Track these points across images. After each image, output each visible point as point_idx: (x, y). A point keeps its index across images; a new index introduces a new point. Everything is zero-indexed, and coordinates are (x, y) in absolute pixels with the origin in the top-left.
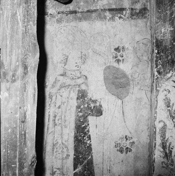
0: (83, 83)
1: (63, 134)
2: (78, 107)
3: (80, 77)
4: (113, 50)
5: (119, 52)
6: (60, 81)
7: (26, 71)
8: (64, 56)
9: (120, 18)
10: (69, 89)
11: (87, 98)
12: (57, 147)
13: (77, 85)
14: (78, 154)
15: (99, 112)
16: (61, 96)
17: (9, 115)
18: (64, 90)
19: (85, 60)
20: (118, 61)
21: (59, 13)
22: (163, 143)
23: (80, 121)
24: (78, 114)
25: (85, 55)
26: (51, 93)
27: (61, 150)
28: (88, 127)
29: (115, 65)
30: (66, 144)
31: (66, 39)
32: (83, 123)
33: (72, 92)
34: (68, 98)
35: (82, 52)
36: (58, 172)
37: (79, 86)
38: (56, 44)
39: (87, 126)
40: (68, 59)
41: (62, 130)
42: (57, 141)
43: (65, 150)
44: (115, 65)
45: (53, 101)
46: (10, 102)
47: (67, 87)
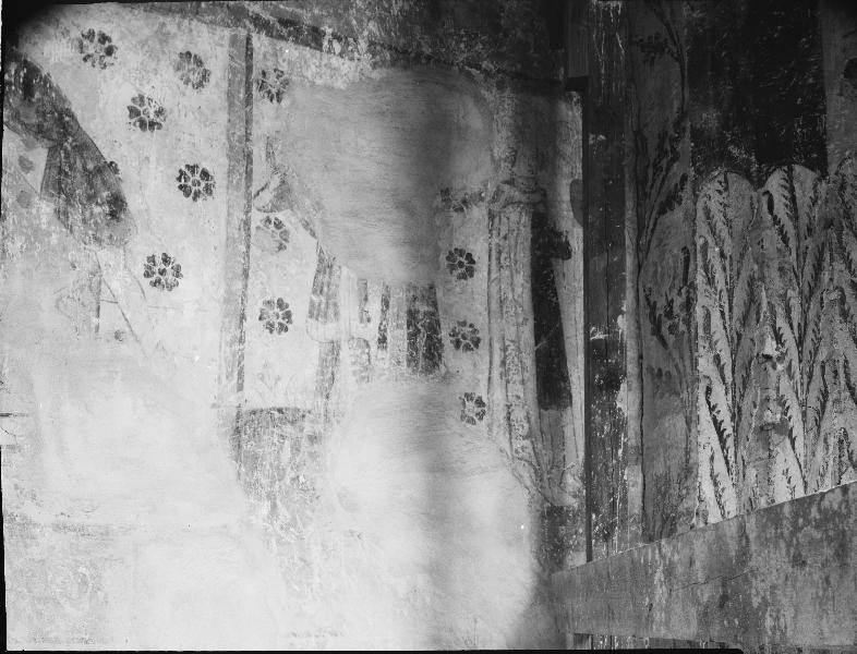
16: (508, 219)
30: (520, 300)
36: (512, 347)
43: (519, 310)
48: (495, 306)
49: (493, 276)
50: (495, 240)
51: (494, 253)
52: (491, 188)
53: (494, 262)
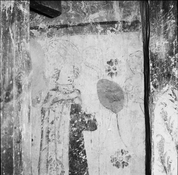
0: (76, 97)
1: (58, 150)
2: (72, 122)
3: (73, 92)
4: (106, 64)
5: (112, 65)
6: (52, 95)
7: (20, 89)
8: (56, 70)
9: (112, 31)
10: (62, 104)
11: (81, 113)
12: (51, 164)
13: (70, 99)
14: (74, 170)
15: (93, 126)
16: (54, 111)
17: (3, 135)
18: (56, 105)
19: (77, 74)
20: (112, 74)
21: (49, 27)
22: (161, 157)
23: (74, 136)
24: (72, 129)
25: (78, 69)
26: (44, 108)
27: (55, 166)
28: (83, 142)
29: (109, 78)
30: (61, 160)
31: (57, 53)
32: (78, 138)
33: (65, 107)
34: (61, 113)
35: (74, 66)
37: (72, 100)
38: (47, 58)
39: (82, 141)
40: (60, 73)
41: (56, 146)
42: (51, 158)
43: (60, 166)
44: (109, 78)
45: (46, 117)
46: (4, 122)
47: (60, 102)
48: (43, 165)
49: (43, 147)
50: (45, 125)
51: (45, 134)
52: (44, 95)
53: (45, 138)
